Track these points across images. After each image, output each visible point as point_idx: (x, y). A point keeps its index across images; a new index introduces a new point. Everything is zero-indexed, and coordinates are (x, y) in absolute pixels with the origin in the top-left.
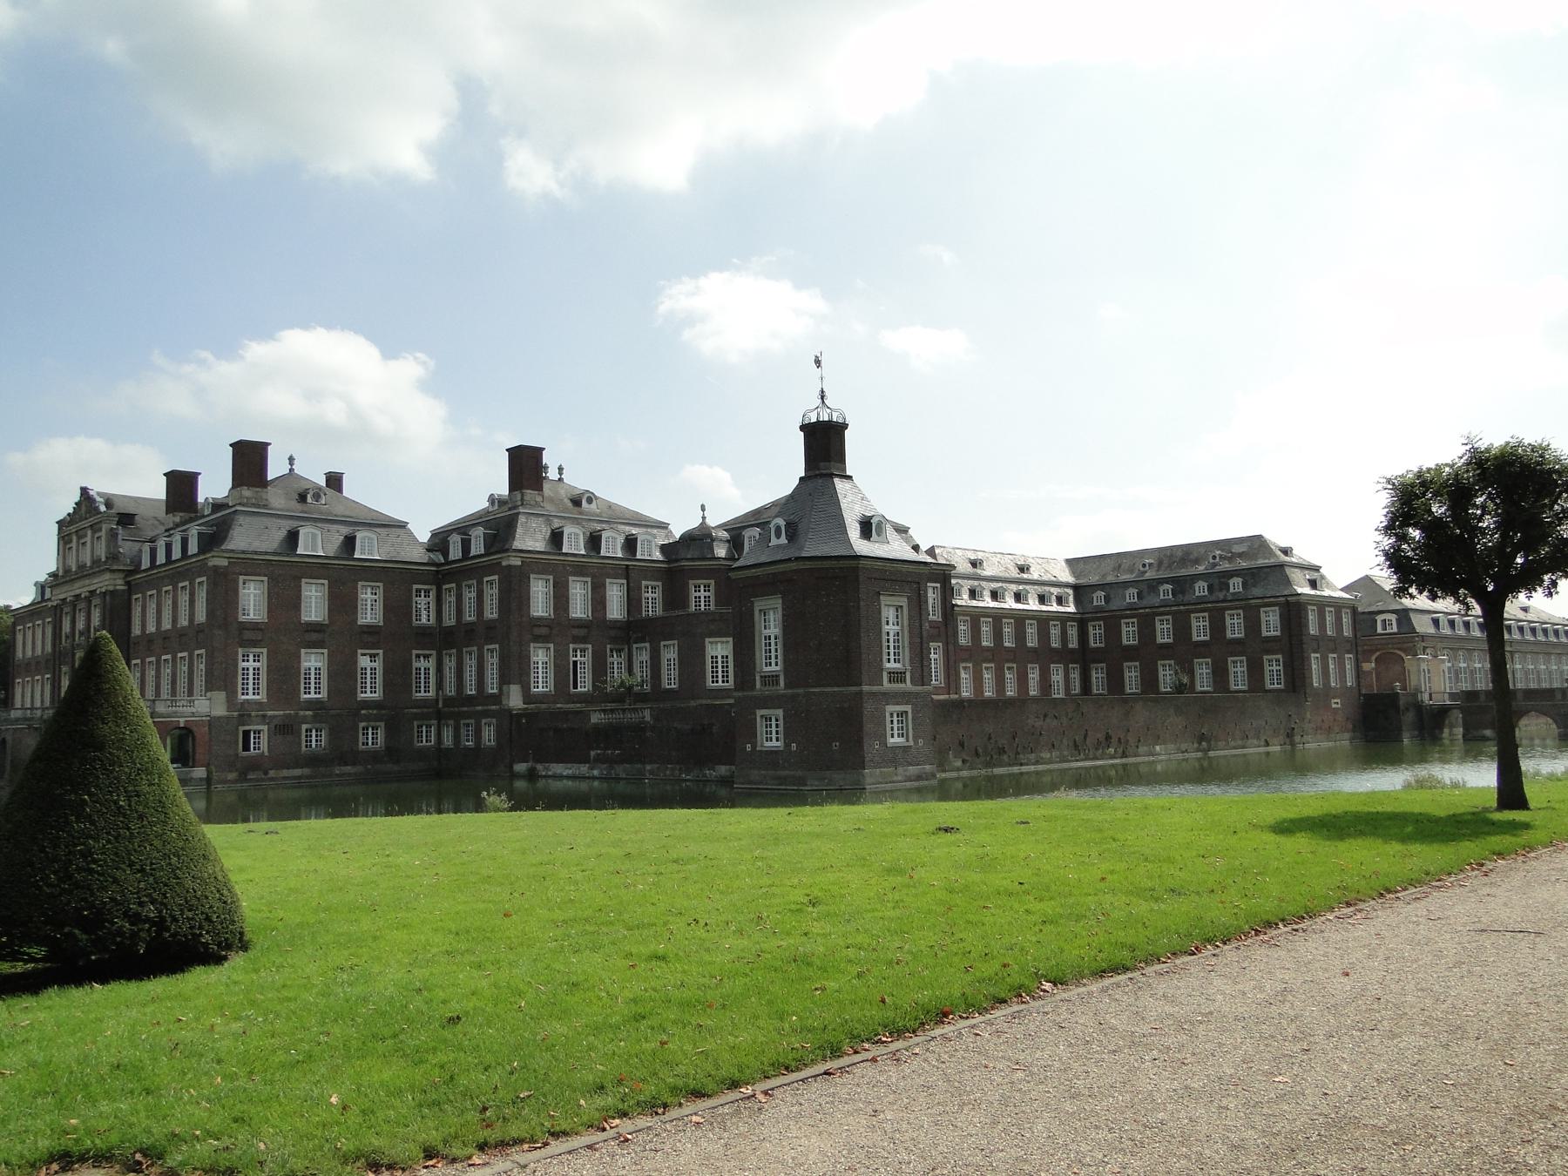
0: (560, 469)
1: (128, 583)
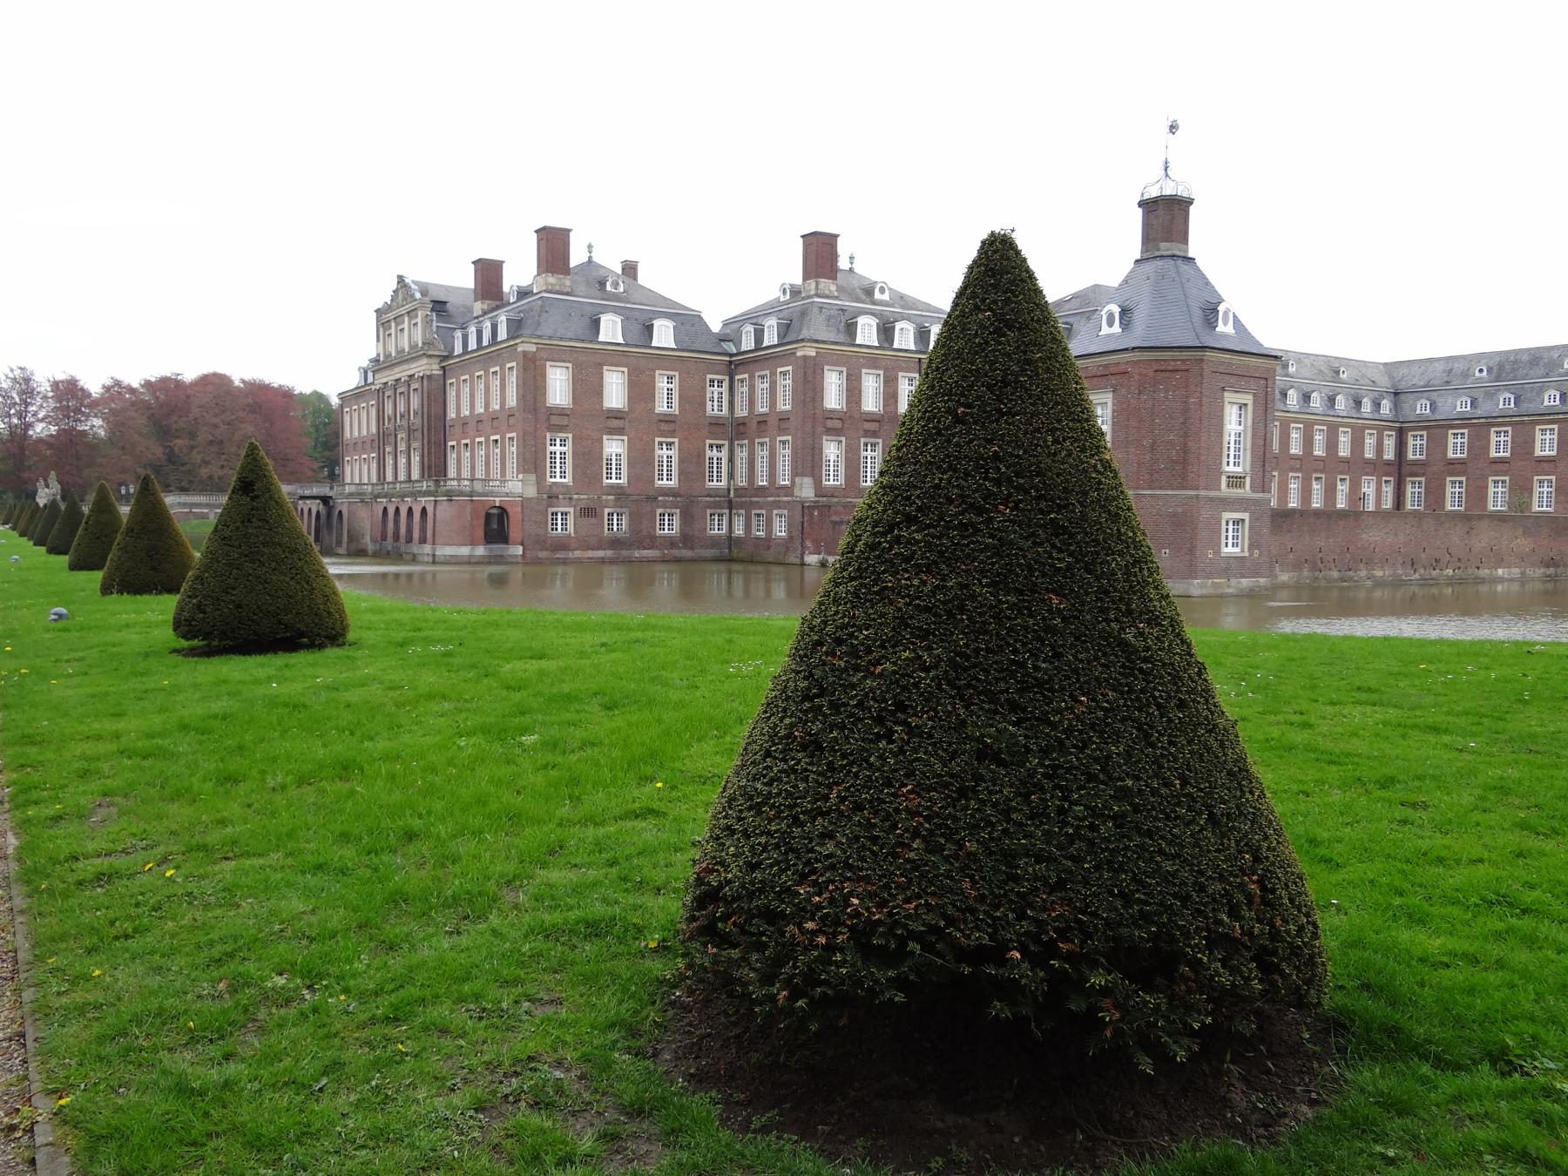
1: (443, 368)
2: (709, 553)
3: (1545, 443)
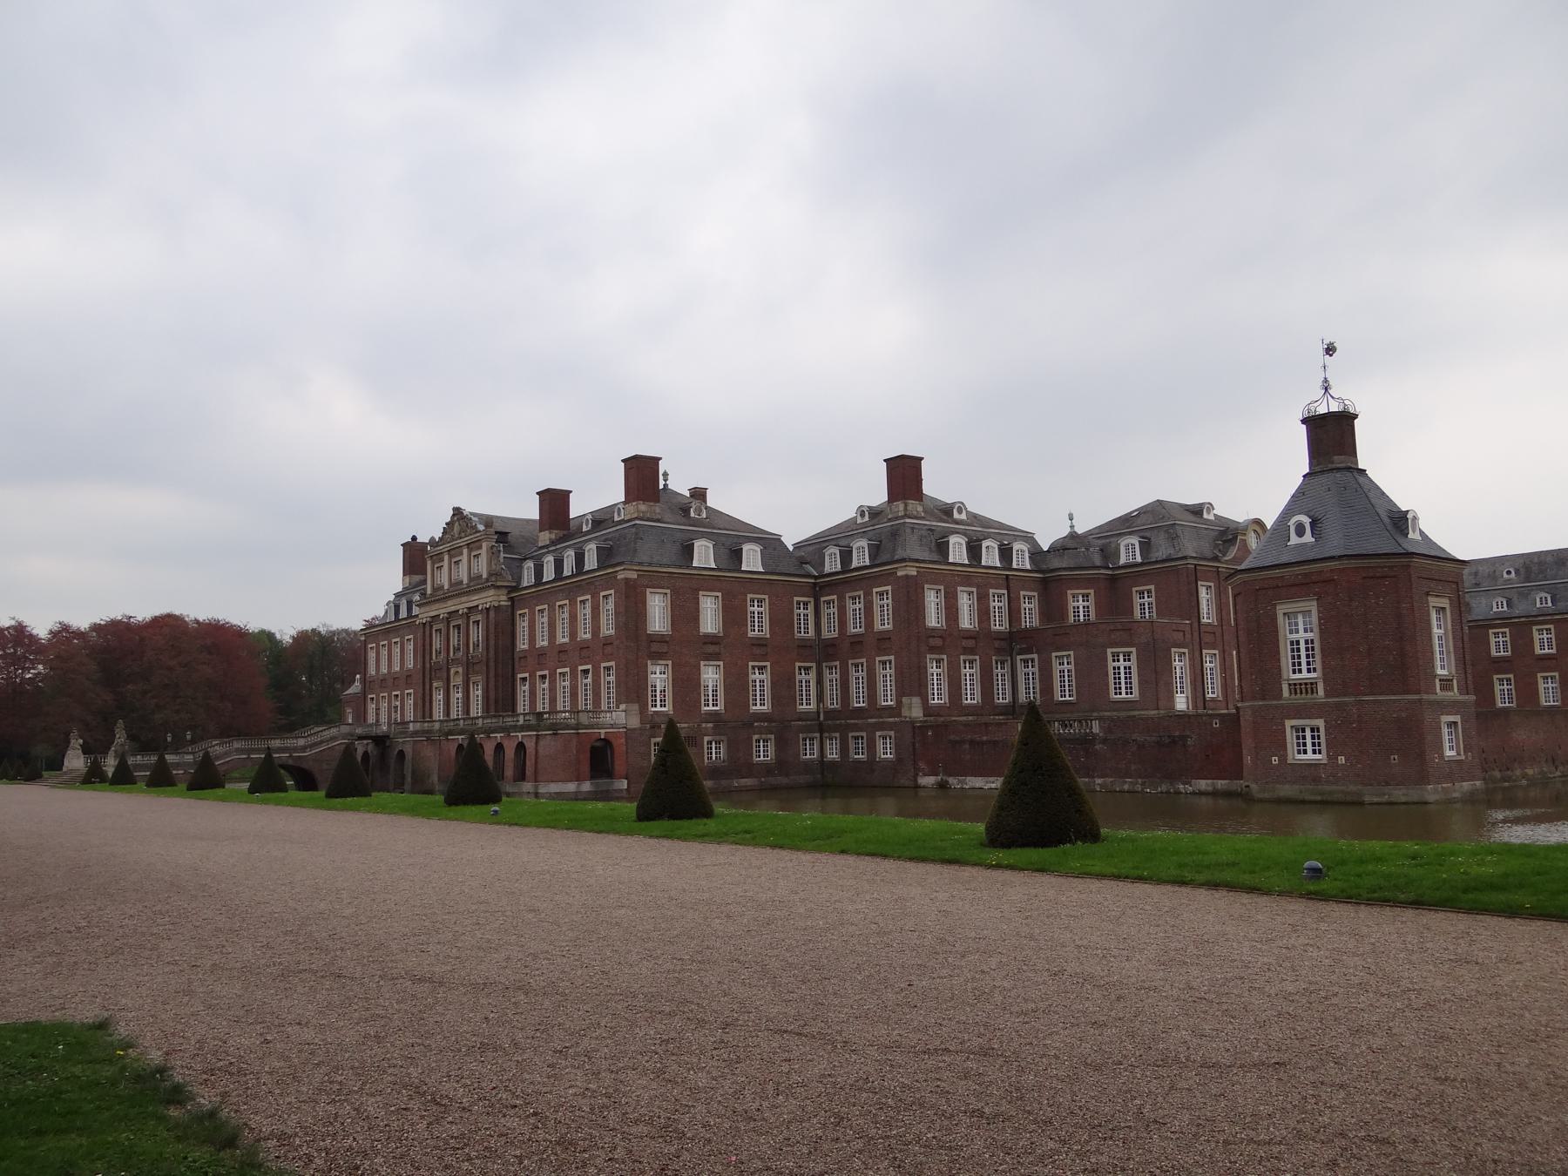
1: (511, 599)
2: (802, 779)
3: (1543, 642)
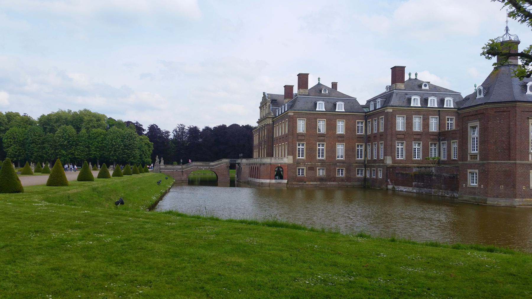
0: (416, 74)
2: (356, 183)
